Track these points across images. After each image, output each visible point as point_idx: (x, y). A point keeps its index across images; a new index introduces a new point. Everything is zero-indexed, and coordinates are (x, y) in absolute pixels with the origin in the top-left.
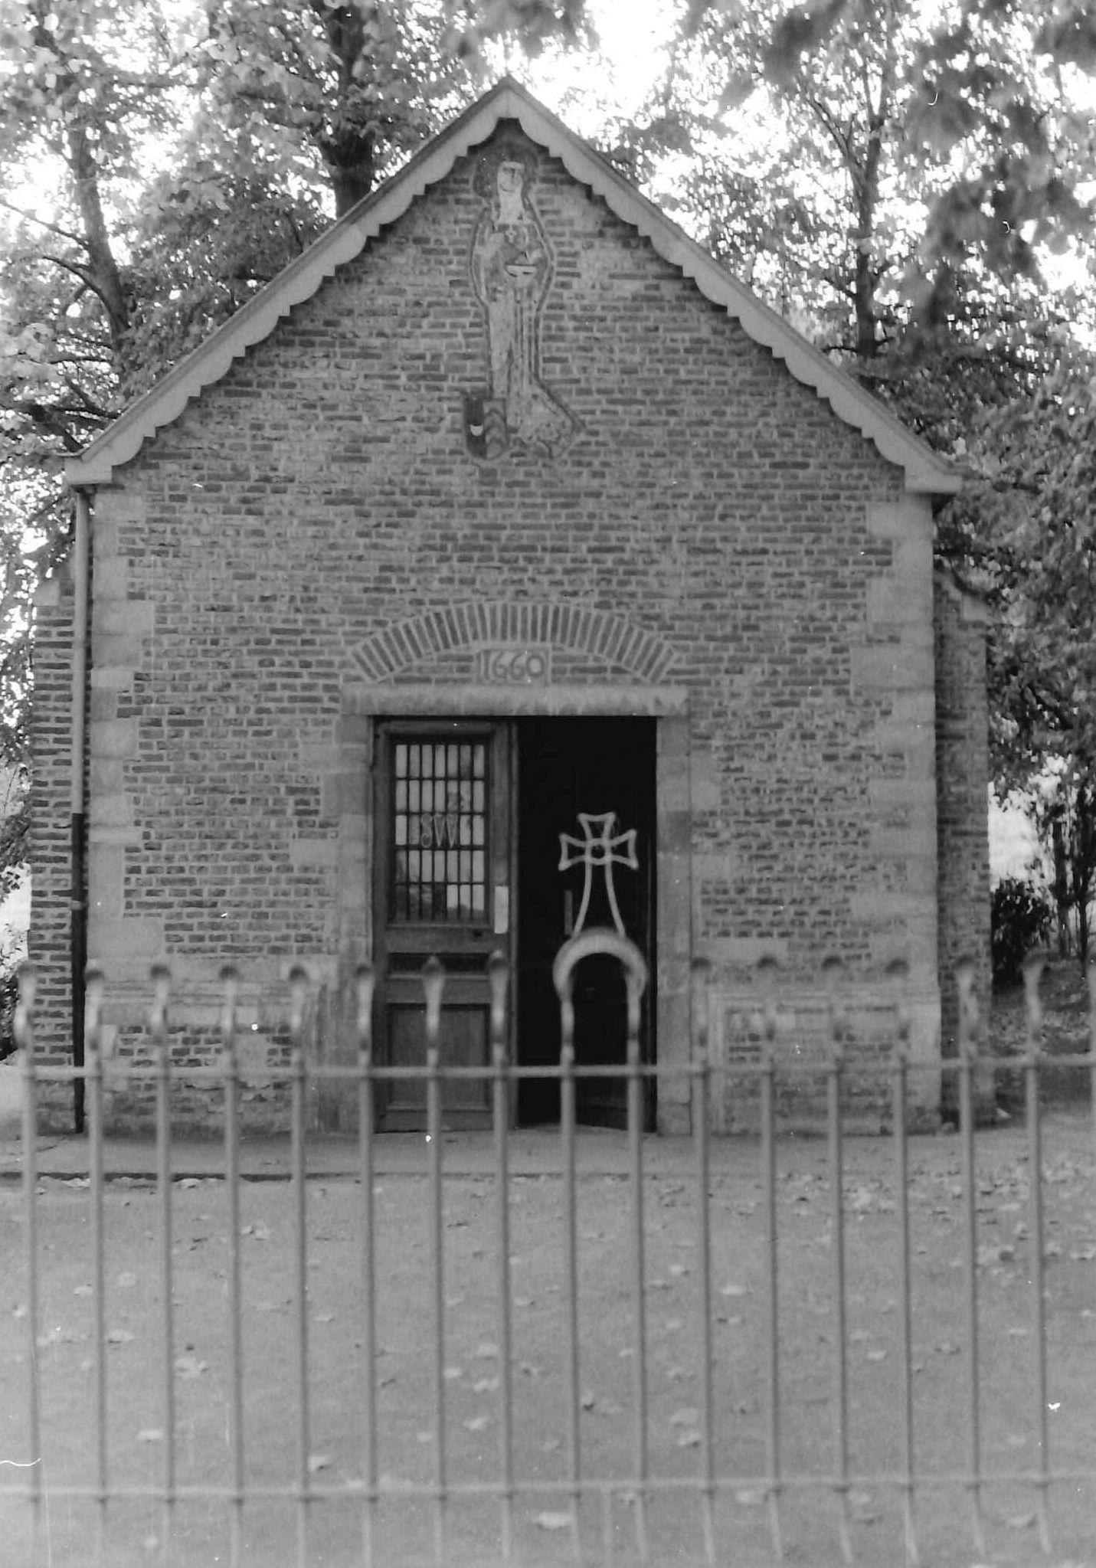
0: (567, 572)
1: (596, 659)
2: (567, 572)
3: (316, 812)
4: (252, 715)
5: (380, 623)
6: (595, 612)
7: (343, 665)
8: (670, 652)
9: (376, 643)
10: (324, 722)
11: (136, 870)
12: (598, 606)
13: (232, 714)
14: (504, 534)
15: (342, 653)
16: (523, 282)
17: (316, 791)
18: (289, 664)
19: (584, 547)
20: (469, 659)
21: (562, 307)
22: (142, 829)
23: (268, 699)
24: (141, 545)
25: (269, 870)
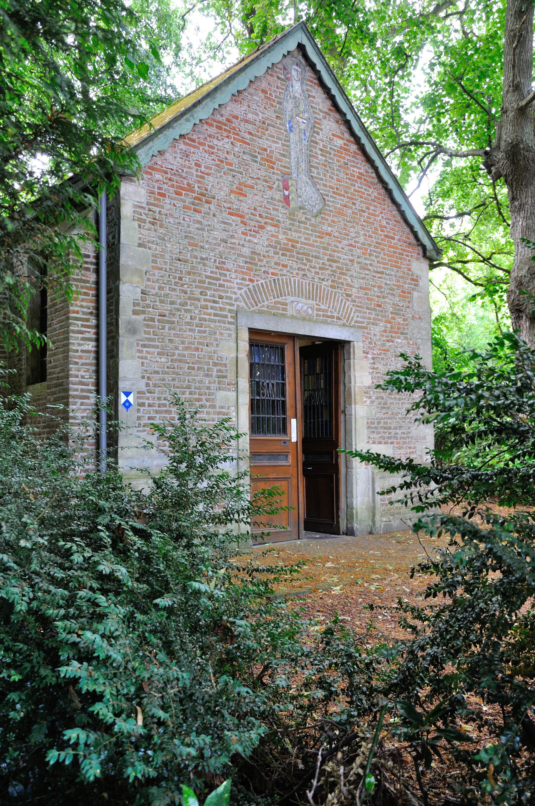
0: (320, 268)
2: (320, 268)
3: (225, 377)
4: (197, 321)
5: (251, 280)
10: (229, 329)
11: (143, 405)
12: (332, 287)
13: (188, 320)
14: (299, 245)
15: (235, 293)
17: (225, 365)
18: (214, 296)
19: (326, 258)
20: (286, 304)
21: (317, 143)
22: (145, 381)
23: (205, 314)
24: (144, 217)
25: (206, 407)
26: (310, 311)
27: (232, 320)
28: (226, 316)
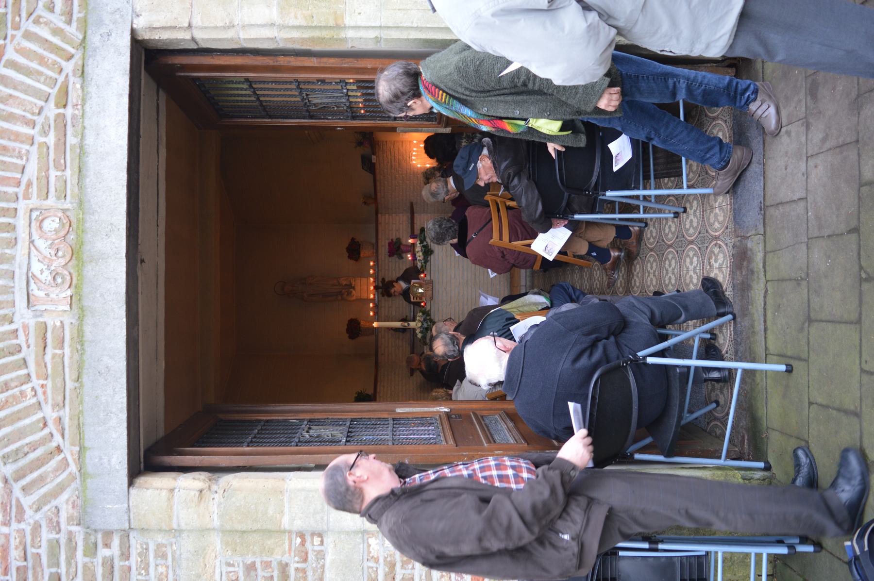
1: (45, 133)
7: (56, 527)
8: (37, 22)
9: (19, 475)
10: (144, 554)
15: (37, 527)
20: (43, 329)
26: (51, 224)
27: (116, 542)
28: (109, 565)
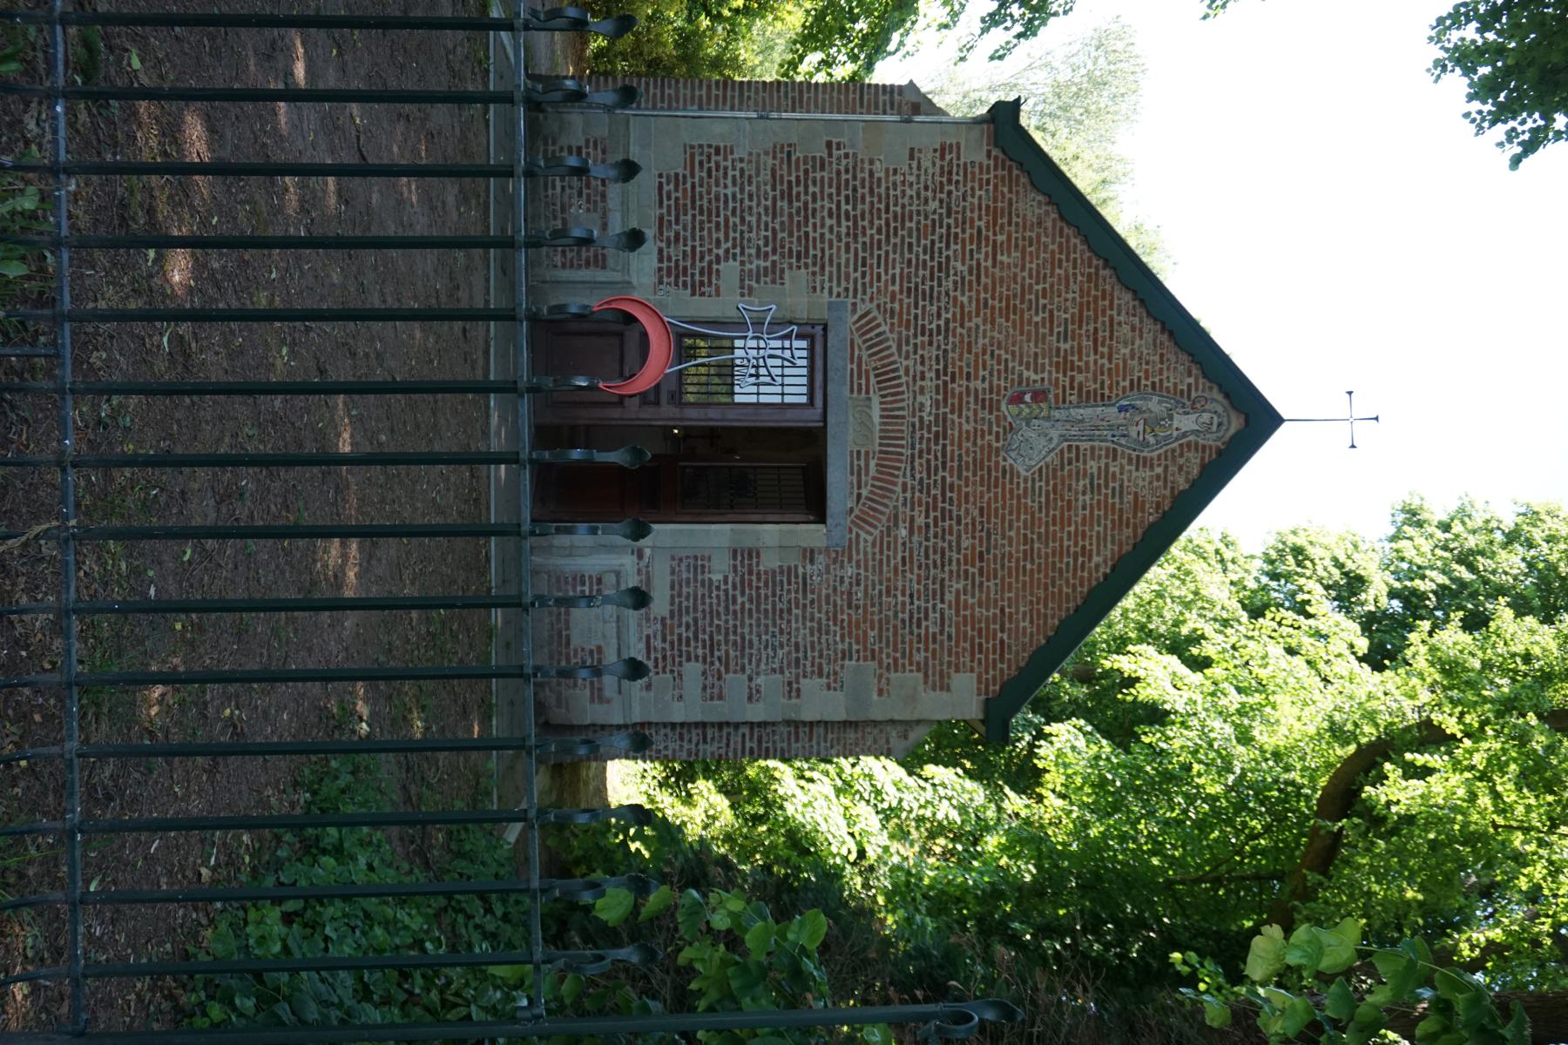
6: (901, 480)
9: (879, 325)
11: (717, 152)
16: (1133, 431)
